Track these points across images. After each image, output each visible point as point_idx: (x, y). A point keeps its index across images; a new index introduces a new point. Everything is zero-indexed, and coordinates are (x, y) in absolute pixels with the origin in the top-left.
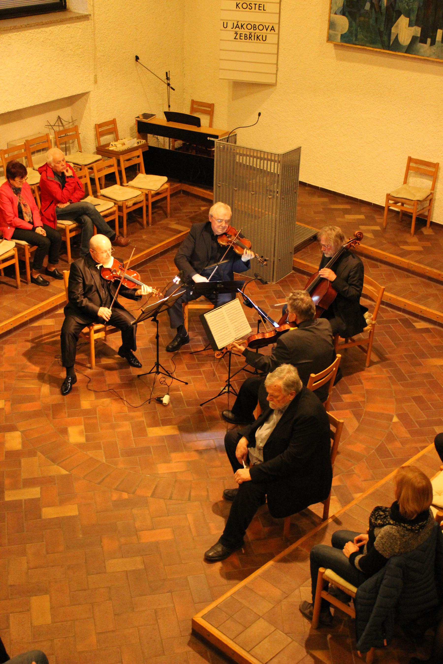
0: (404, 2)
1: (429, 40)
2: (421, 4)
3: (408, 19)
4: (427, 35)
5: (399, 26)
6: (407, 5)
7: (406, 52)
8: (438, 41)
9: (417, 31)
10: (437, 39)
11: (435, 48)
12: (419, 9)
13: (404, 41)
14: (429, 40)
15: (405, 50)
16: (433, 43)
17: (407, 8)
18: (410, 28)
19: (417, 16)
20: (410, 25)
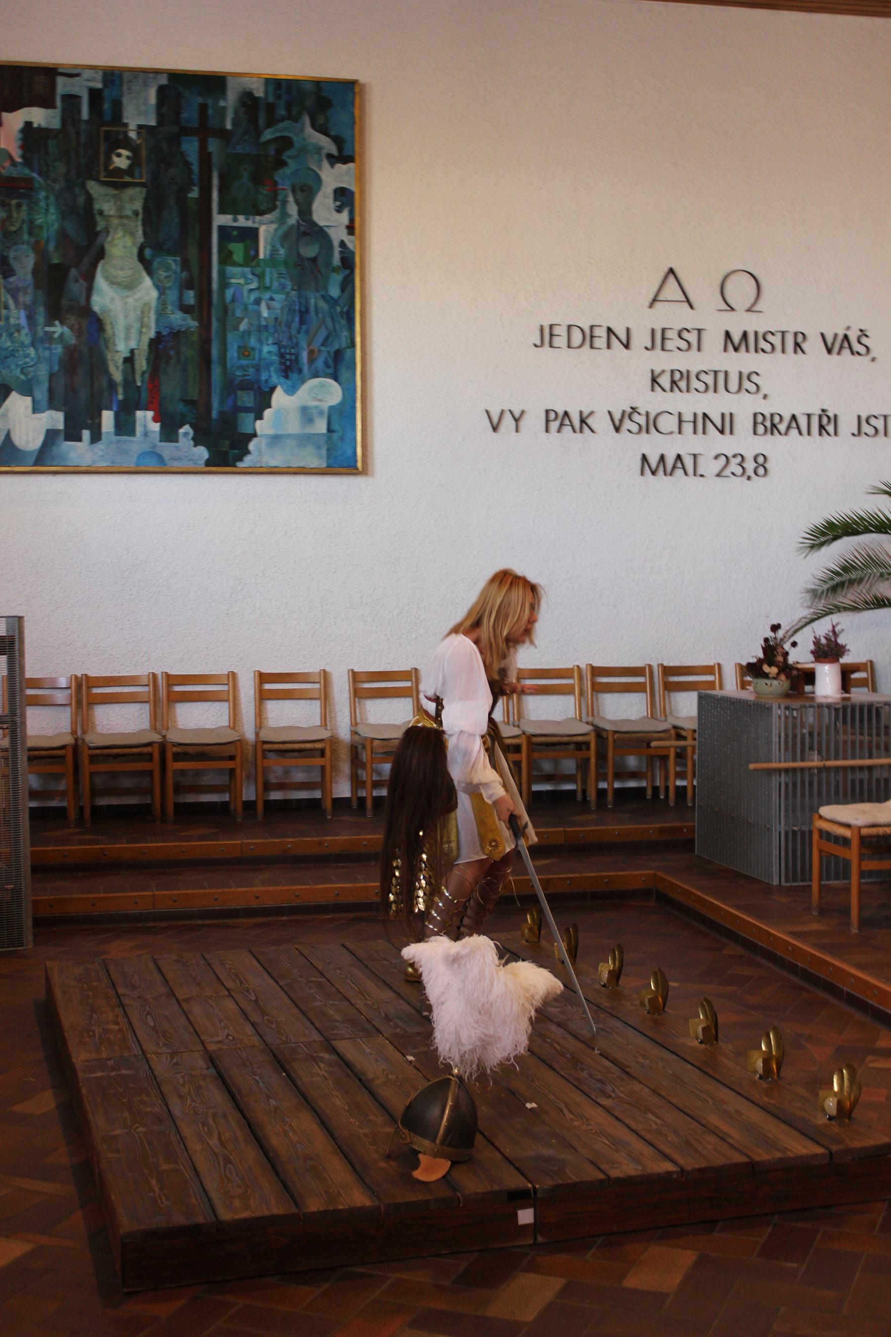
0: (13, 367)
1: (86, 434)
2: (56, 368)
3: (29, 399)
4: (79, 423)
5: (10, 414)
6: (22, 372)
7: (35, 465)
8: (108, 433)
9: (56, 419)
10: (105, 429)
11: (102, 447)
12: (51, 377)
13: (27, 442)
14: (86, 434)
15: (32, 459)
16: (96, 437)
17: (23, 377)
18: (38, 415)
19: (51, 391)
20: (35, 410)
